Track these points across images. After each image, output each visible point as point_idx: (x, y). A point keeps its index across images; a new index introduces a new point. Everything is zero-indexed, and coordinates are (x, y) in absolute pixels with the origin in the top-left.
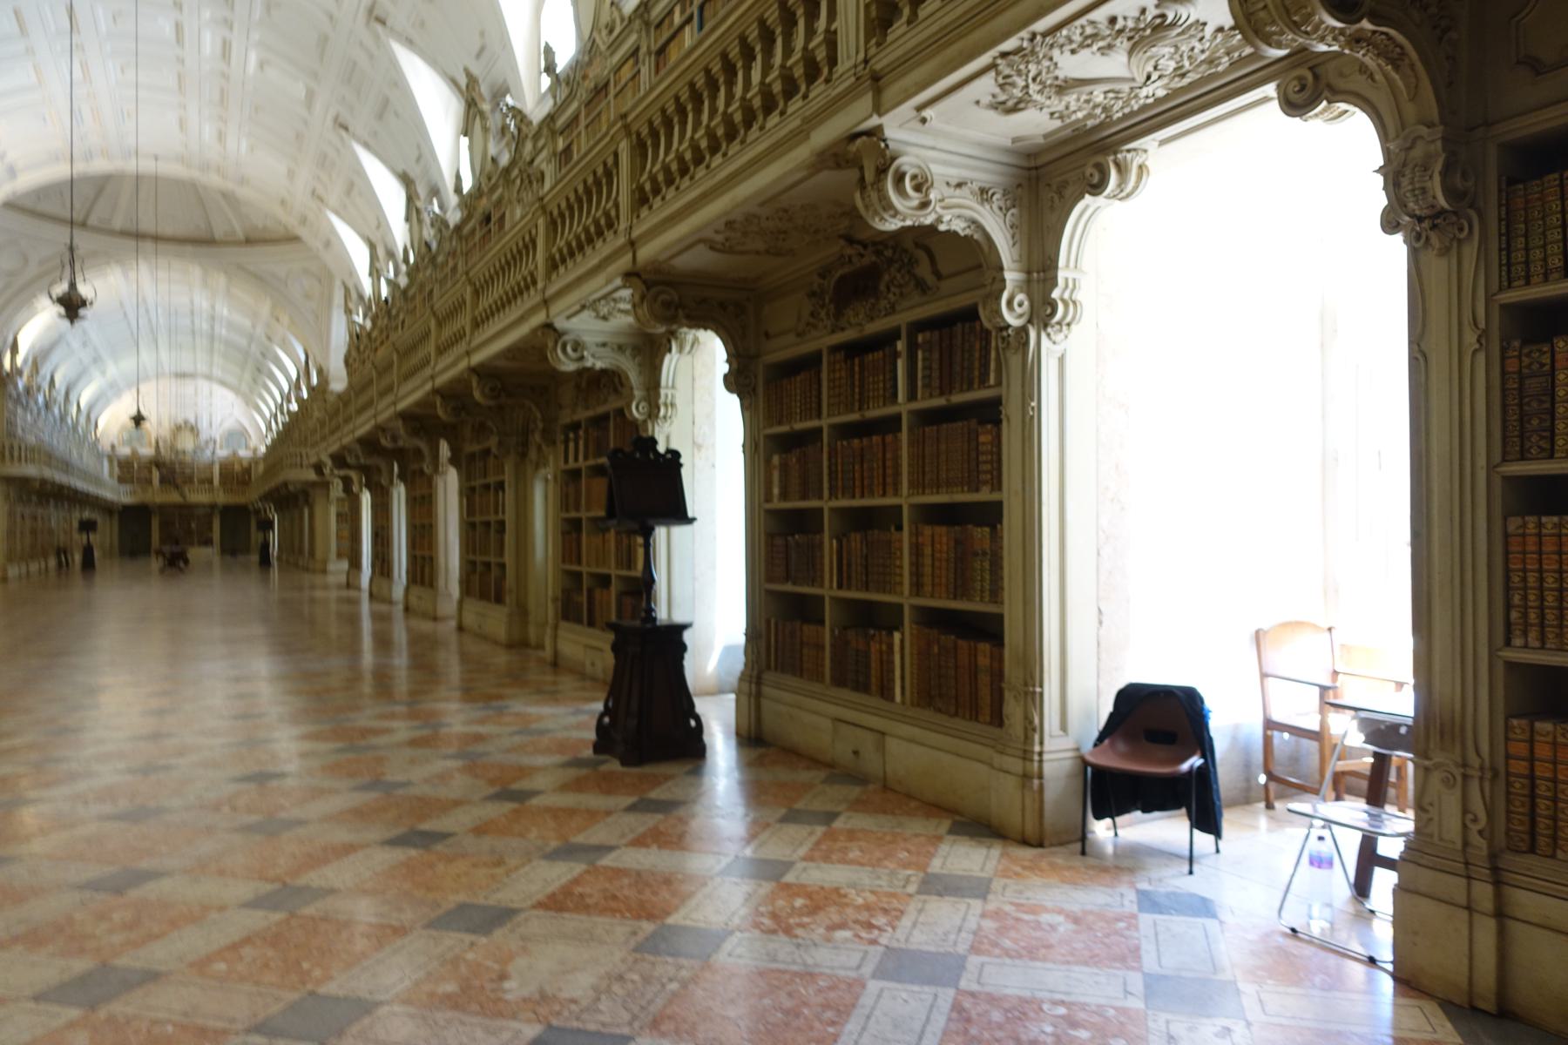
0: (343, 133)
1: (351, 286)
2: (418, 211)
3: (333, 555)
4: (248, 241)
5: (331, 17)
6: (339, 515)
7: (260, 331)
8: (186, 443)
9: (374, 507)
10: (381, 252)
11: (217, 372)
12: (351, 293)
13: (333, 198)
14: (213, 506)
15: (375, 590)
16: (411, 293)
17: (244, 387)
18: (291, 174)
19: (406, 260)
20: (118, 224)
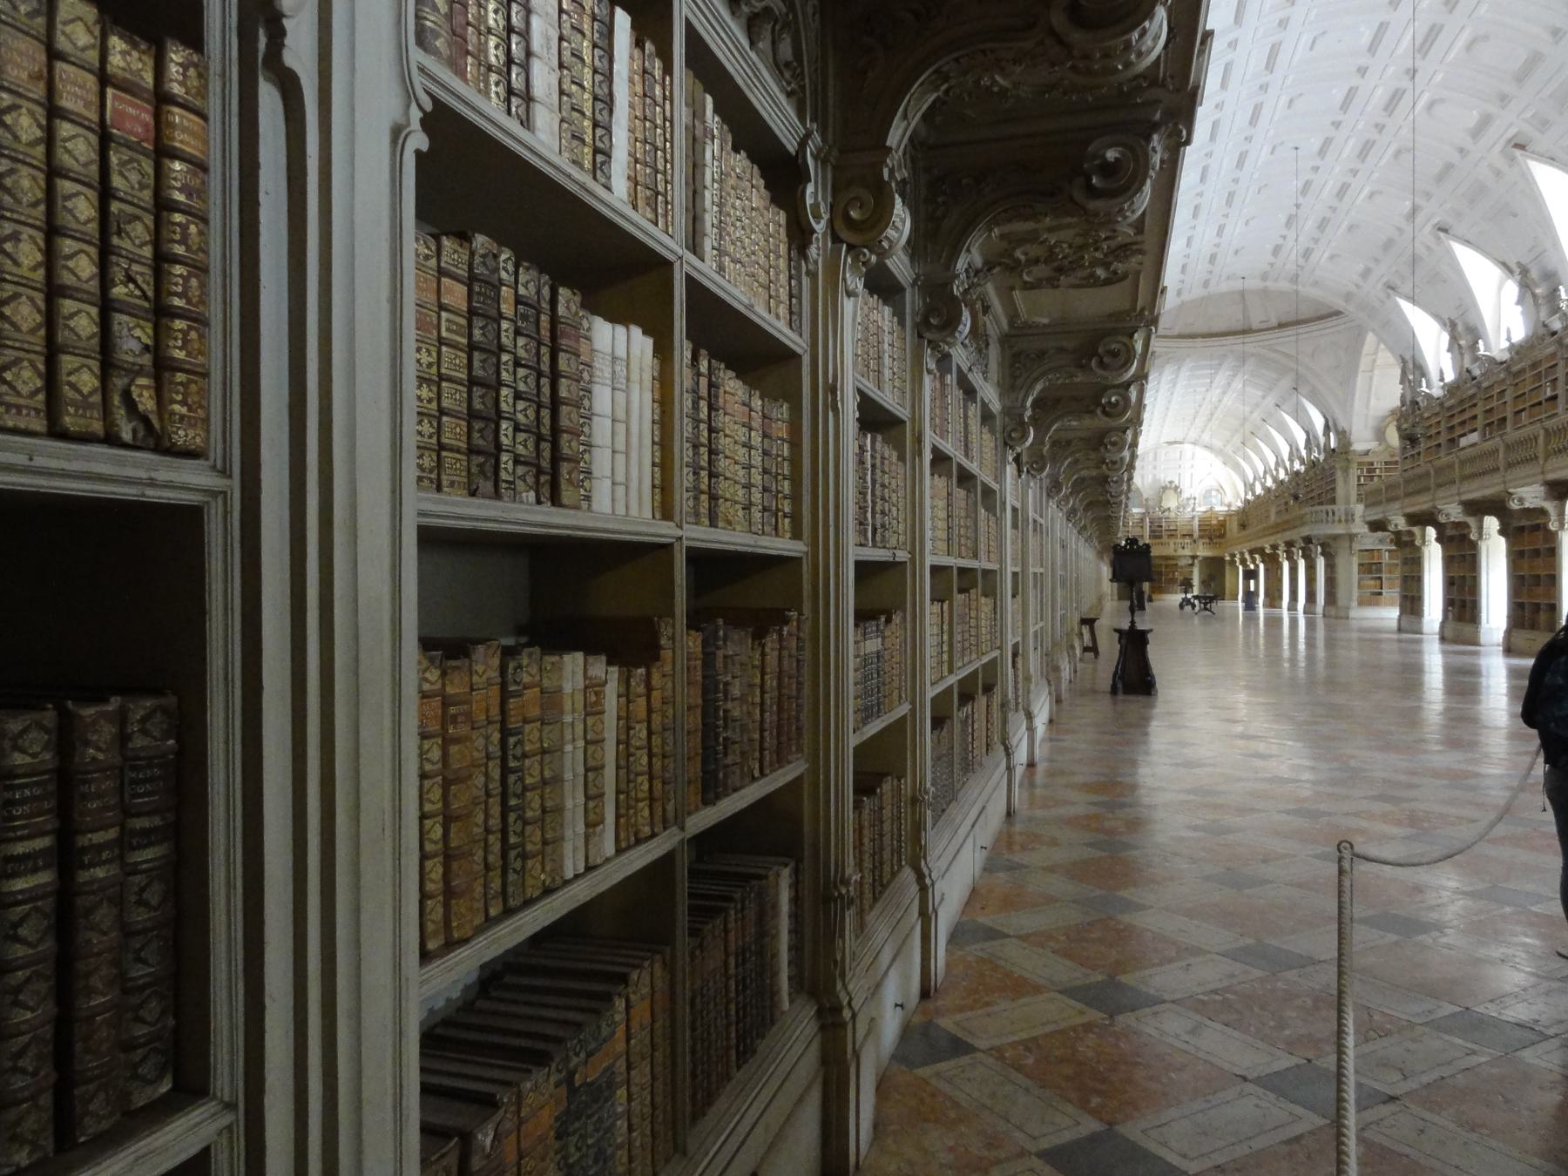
0: (1442, 234)
1: (1408, 357)
2: (1534, 296)
3: (1355, 604)
4: (1281, 326)
5: (1461, 150)
6: (1361, 565)
7: (1270, 400)
8: (1171, 502)
9: (1448, 561)
10: (1460, 328)
11: (1206, 437)
12: (1413, 368)
13: (1406, 288)
14: (1194, 557)
15: (1448, 634)
16: (1515, 369)
17: (1229, 449)
18: (1366, 273)
19: (1509, 339)
20: (1176, 332)
